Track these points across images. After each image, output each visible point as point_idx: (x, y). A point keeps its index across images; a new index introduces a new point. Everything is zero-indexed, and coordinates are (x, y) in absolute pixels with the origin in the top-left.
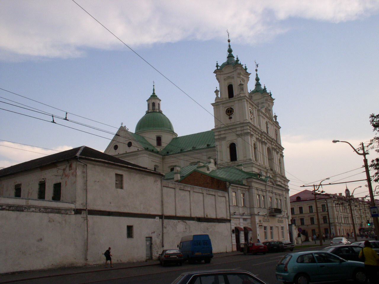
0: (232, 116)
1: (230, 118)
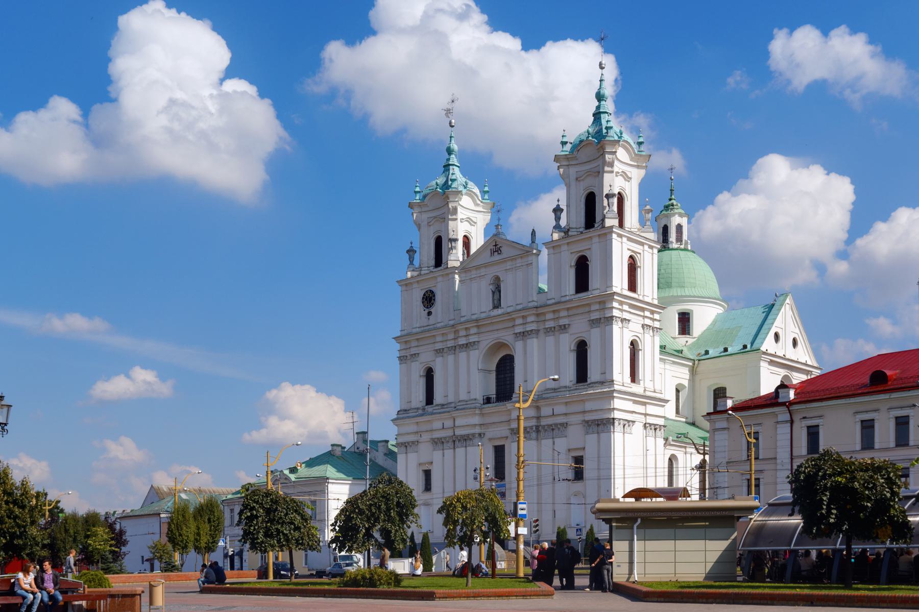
1: (429, 314)
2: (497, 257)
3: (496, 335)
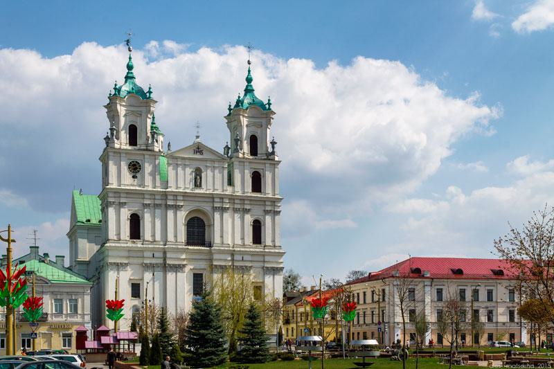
0: (138, 175)
2: (198, 156)
3: (197, 204)
